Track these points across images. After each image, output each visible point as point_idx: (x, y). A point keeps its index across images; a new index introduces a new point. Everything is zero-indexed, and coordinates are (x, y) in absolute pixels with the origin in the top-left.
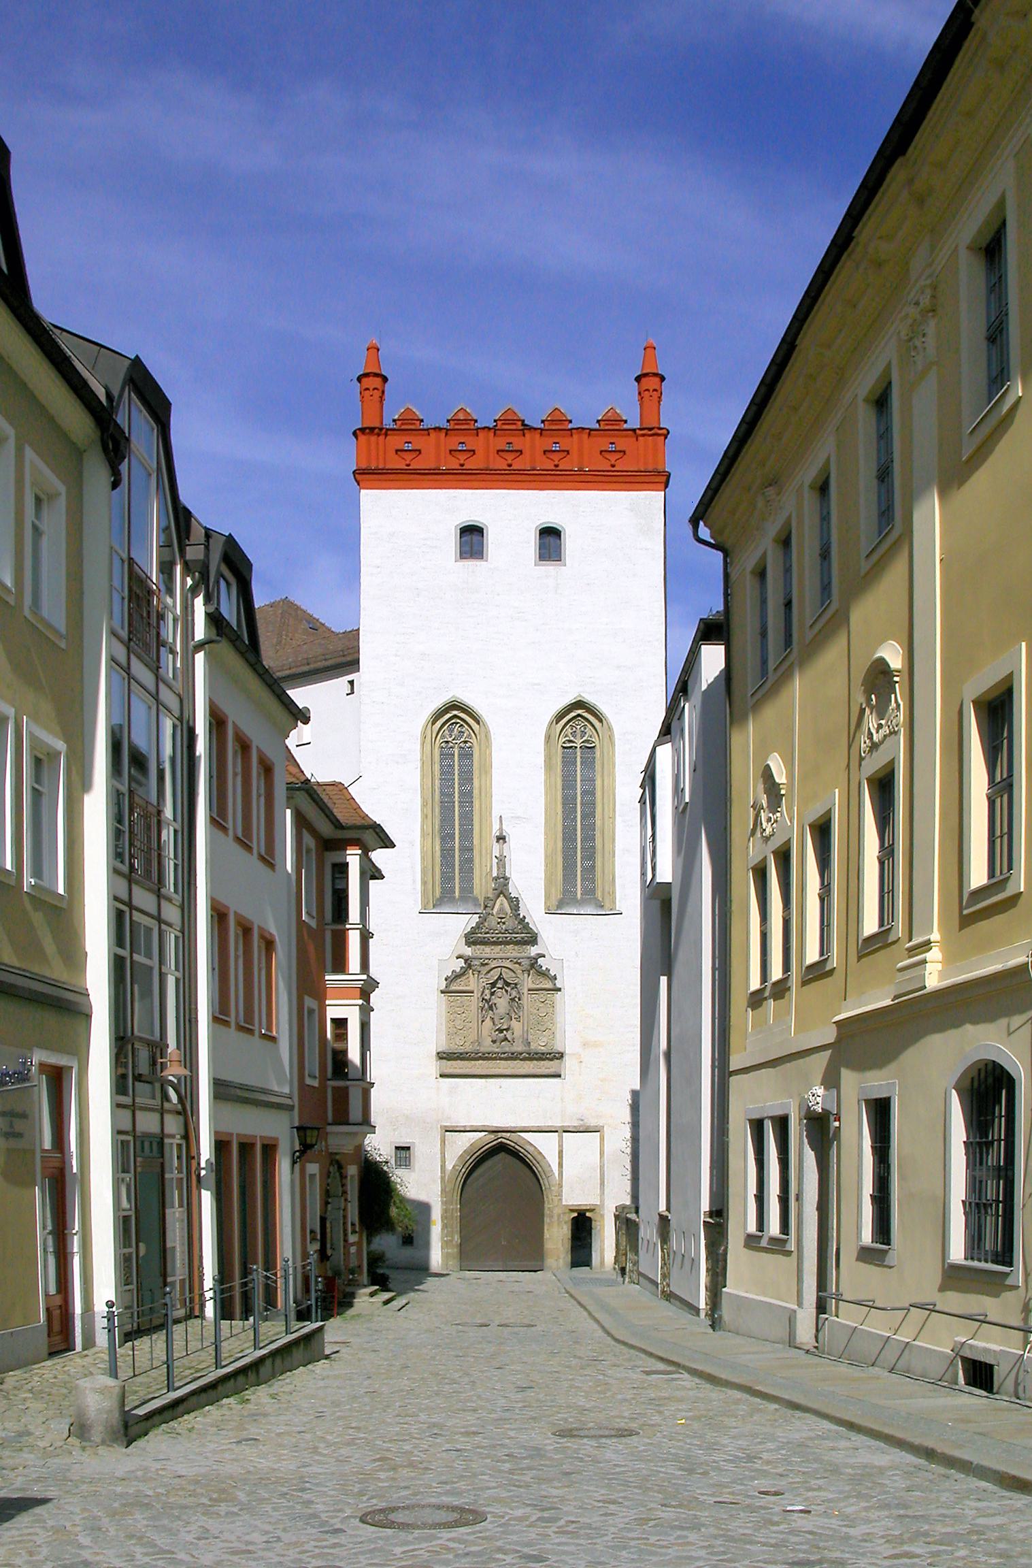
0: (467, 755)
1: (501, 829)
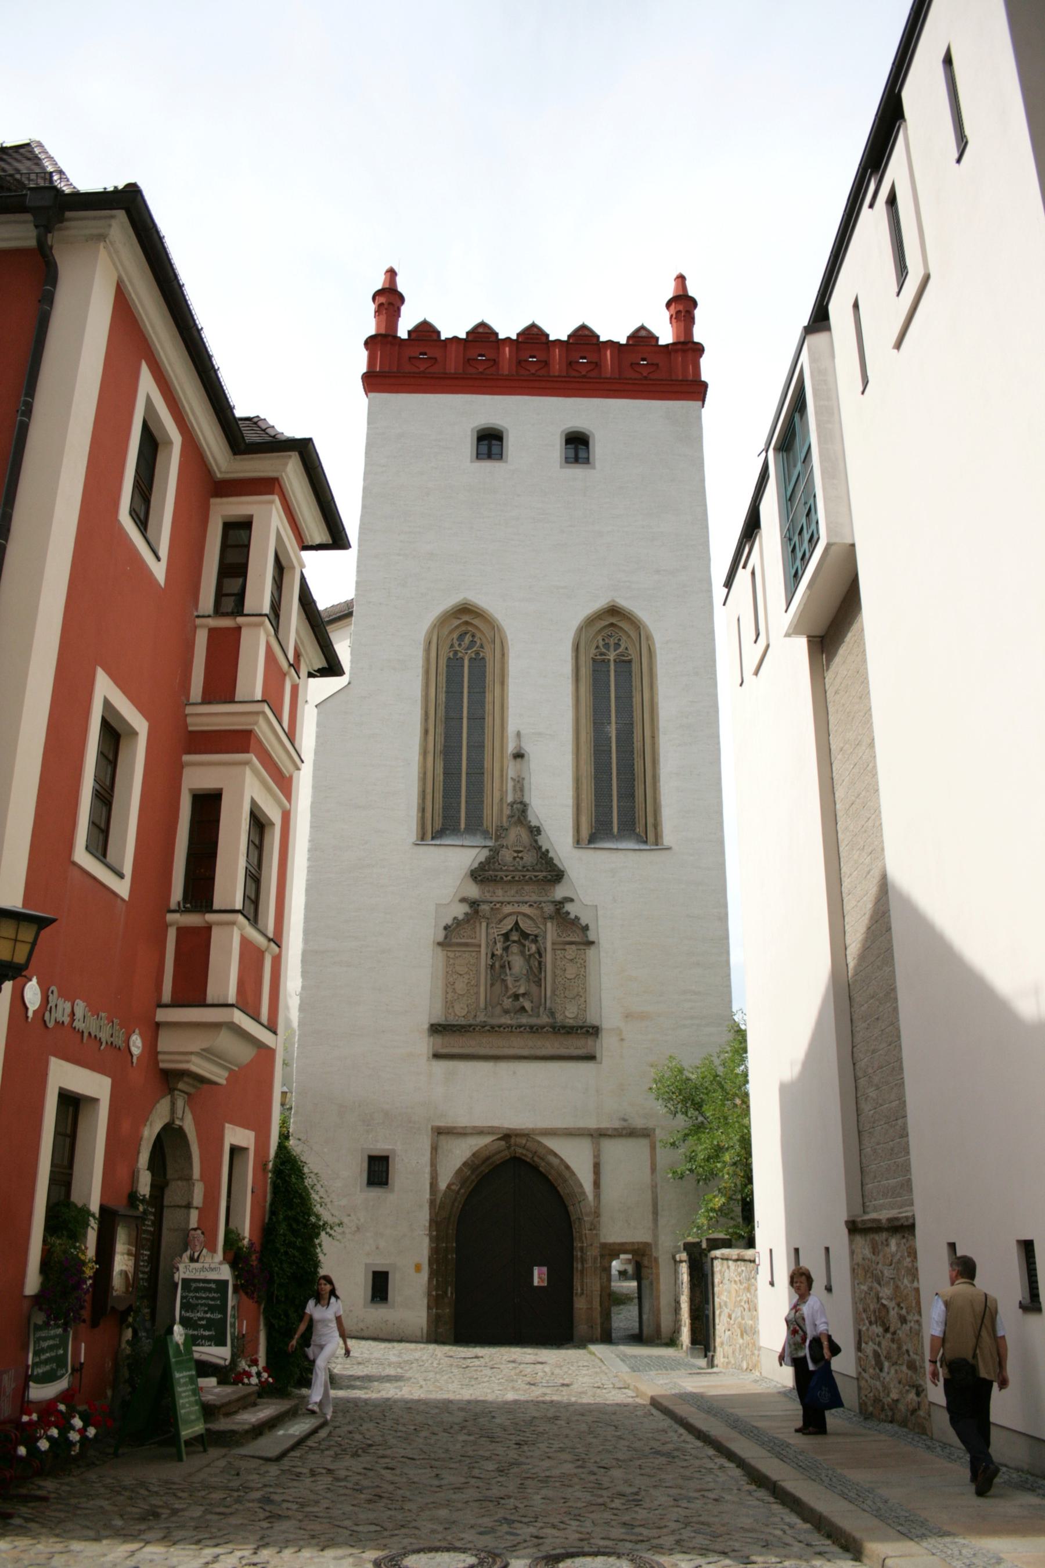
0: (479, 663)
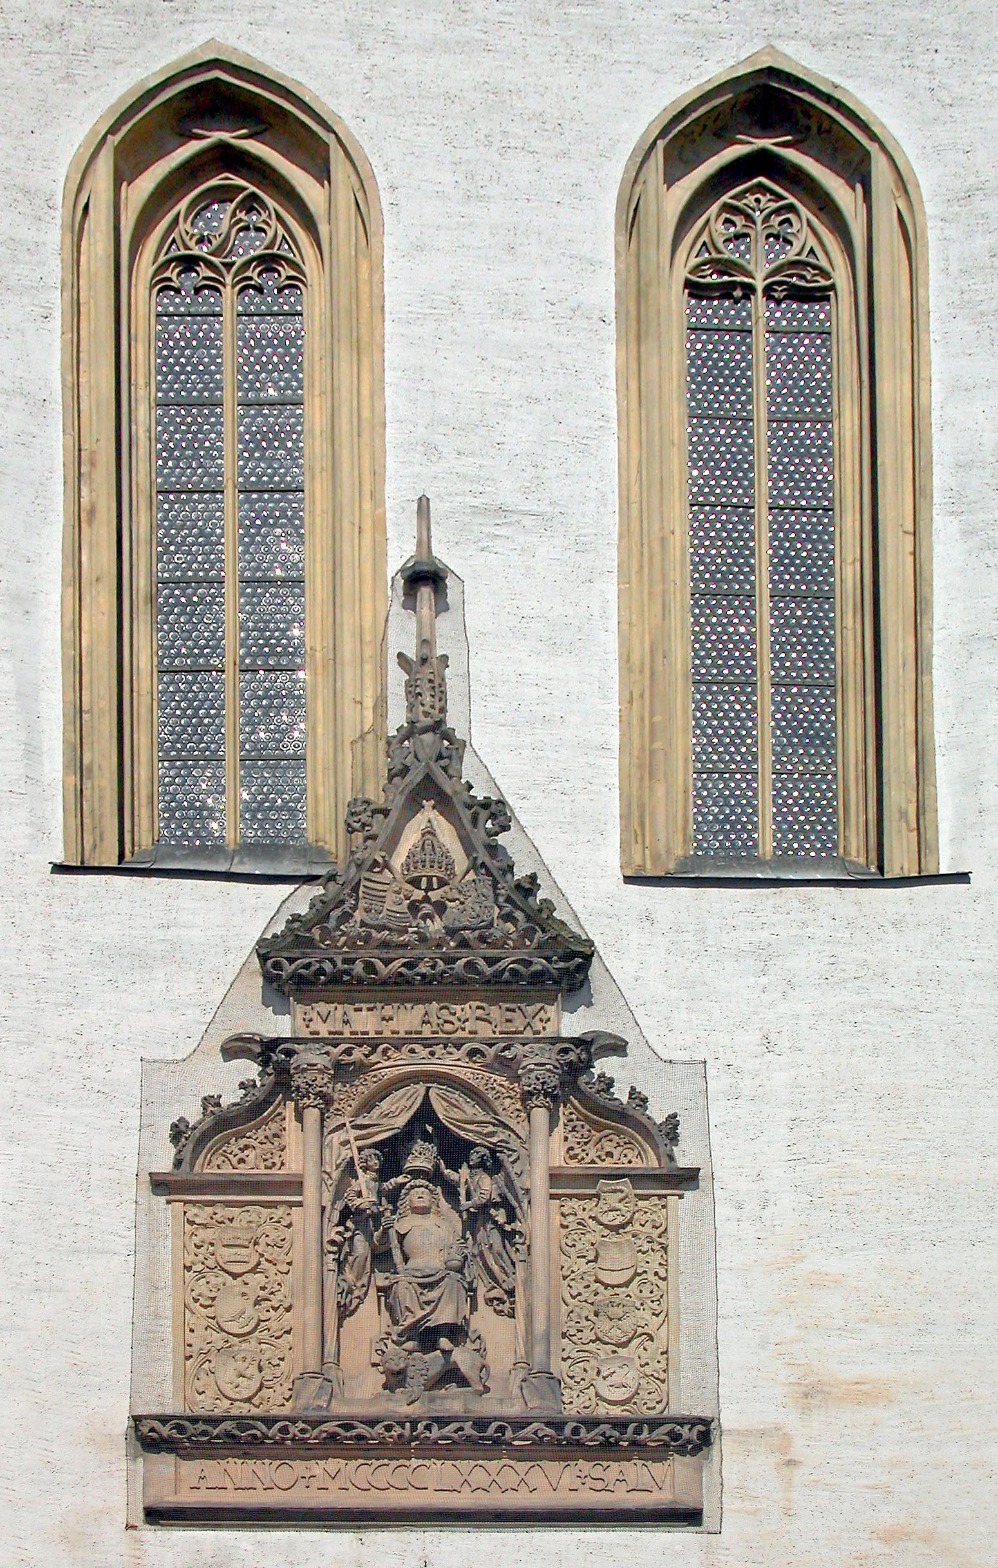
1: (424, 543)
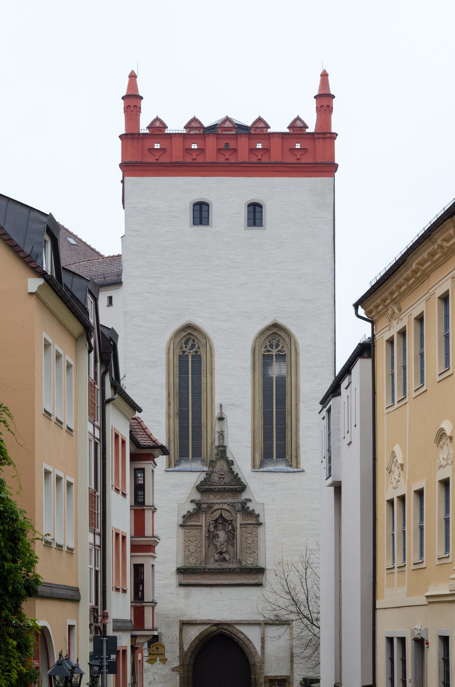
0: (197, 359)
